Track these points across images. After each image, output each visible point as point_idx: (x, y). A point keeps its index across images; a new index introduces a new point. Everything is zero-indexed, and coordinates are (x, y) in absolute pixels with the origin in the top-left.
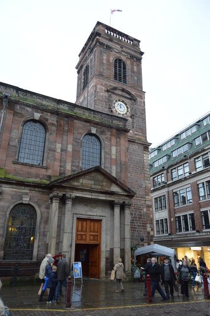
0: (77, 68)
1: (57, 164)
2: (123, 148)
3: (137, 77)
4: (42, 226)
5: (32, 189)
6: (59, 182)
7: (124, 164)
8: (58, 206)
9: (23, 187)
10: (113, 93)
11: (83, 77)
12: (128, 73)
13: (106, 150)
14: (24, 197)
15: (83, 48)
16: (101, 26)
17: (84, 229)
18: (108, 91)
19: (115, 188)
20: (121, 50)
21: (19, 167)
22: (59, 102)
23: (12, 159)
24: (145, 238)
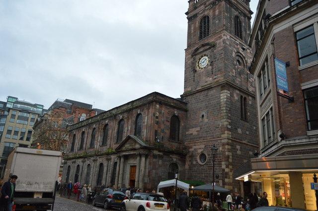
10: (195, 55)
24: (220, 175)
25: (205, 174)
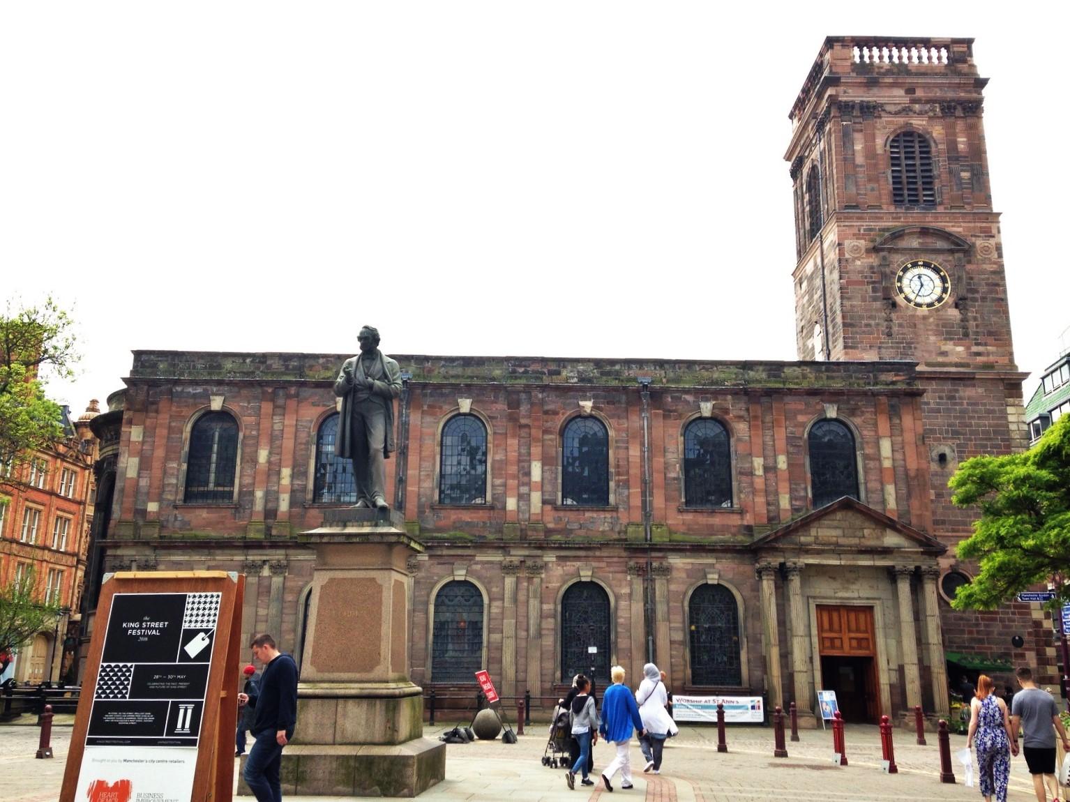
0: (788, 158)
1: (760, 500)
2: (909, 437)
3: (972, 169)
4: (749, 625)
5: (721, 555)
6: (770, 541)
7: (917, 476)
8: (773, 586)
9: (704, 554)
10: (890, 250)
11: (807, 209)
12: (940, 167)
13: (867, 451)
14: (709, 573)
15: (799, 99)
16: (837, 47)
17: (836, 626)
18: (875, 250)
19: (891, 539)
20: (907, 100)
21: (689, 517)
22: (746, 365)
23: (677, 504)
24: (1026, 638)
25: (971, 632)
